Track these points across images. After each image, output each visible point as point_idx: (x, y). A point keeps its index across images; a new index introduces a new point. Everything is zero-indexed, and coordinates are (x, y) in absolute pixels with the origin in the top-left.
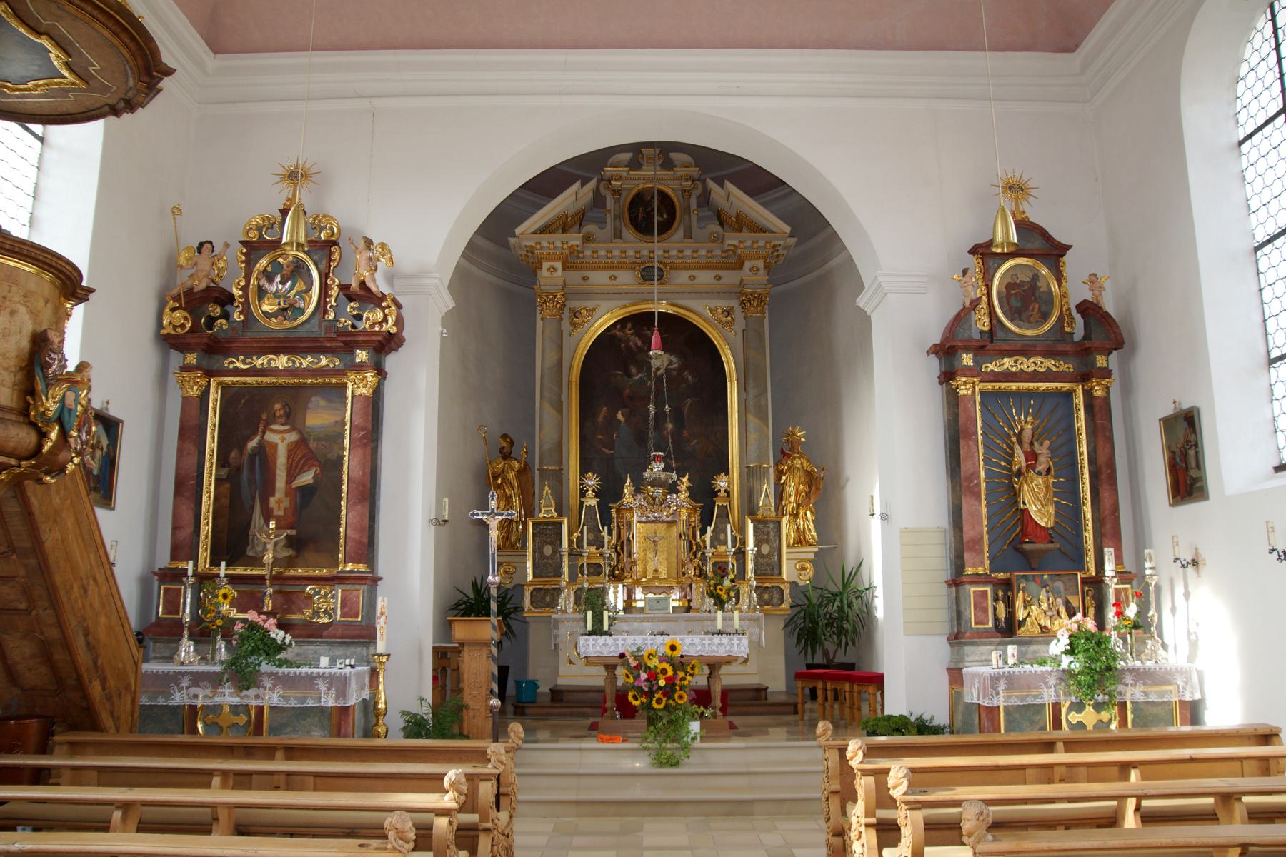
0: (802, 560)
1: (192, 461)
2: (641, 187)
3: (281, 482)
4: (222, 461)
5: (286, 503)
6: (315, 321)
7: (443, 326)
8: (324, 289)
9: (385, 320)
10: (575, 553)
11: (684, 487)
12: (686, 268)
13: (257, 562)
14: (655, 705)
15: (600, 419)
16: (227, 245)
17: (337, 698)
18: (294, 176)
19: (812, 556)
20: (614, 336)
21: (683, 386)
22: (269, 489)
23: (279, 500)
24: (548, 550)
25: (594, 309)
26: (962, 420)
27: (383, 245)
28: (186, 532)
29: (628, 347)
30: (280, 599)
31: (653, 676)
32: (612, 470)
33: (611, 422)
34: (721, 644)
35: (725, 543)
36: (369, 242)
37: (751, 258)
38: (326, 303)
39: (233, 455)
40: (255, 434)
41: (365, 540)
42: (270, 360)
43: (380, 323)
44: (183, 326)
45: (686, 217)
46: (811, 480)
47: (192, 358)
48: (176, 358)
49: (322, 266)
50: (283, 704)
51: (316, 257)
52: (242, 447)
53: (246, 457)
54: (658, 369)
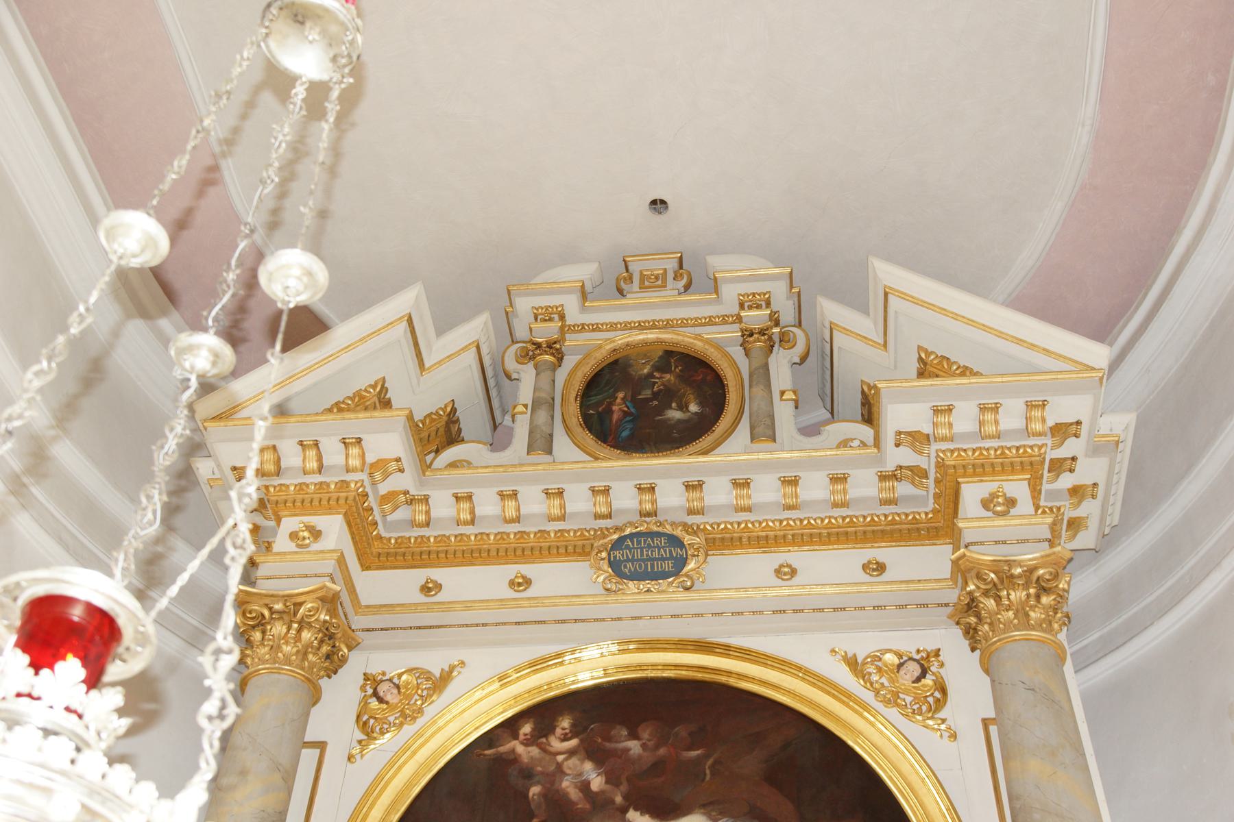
2: (622, 339)
12: (764, 541)
20: (511, 760)
29: (555, 800)
37: (981, 469)
45: (759, 391)
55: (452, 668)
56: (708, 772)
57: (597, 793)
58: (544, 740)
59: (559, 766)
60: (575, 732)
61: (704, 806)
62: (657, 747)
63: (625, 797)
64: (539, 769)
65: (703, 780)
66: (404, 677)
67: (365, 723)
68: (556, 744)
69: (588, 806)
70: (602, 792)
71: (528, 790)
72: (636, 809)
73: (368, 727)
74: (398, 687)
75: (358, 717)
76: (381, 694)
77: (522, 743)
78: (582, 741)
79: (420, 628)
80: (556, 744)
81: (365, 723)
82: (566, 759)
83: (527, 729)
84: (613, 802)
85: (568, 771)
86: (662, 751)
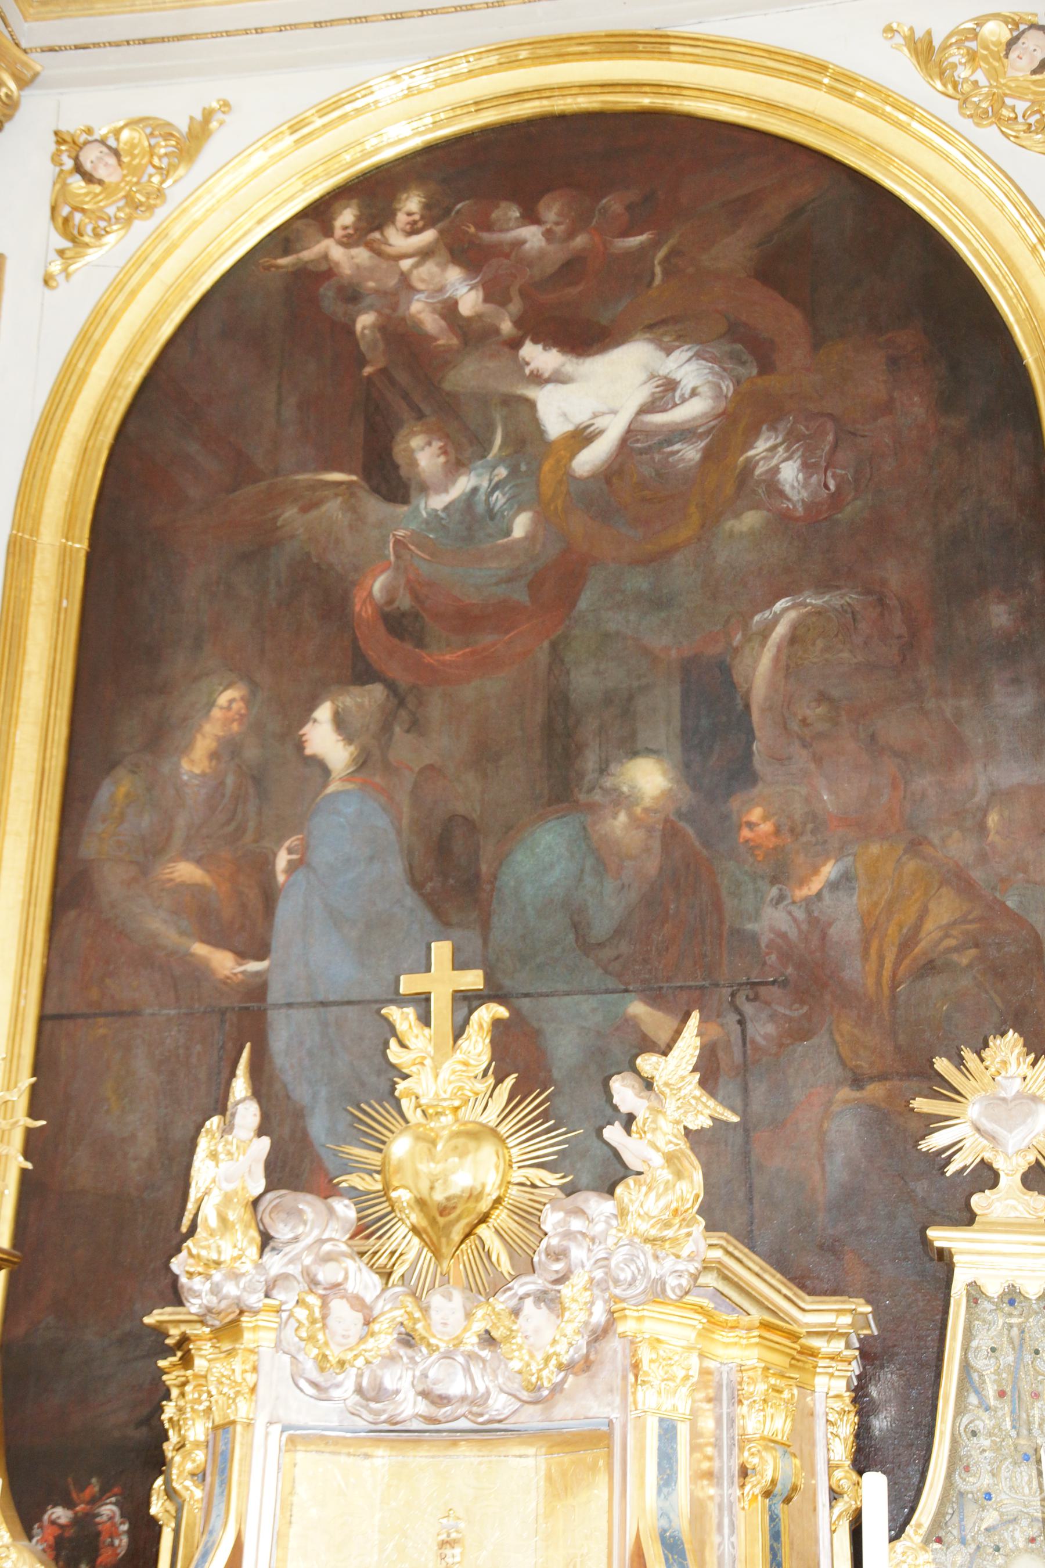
15: (195, 761)
20: (322, 273)
21: (751, 520)
25: (199, 133)
29: (401, 336)
33: (269, 780)
55: (208, 114)
56: (658, 270)
57: (469, 320)
58: (377, 235)
59: (405, 279)
60: (431, 216)
61: (650, 327)
62: (571, 235)
63: (518, 323)
64: (371, 284)
65: (650, 284)
66: (125, 135)
67: (66, 220)
68: (397, 240)
69: (455, 341)
70: (479, 316)
71: (354, 322)
72: (535, 341)
73: (72, 229)
74: (116, 153)
75: (54, 209)
76: (88, 166)
77: (341, 243)
78: (441, 232)
79: (144, 42)
81: (66, 220)
82: (416, 266)
83: (346, 217)
84: (497, 331)
85: (420, 286)
86: (580, 241)
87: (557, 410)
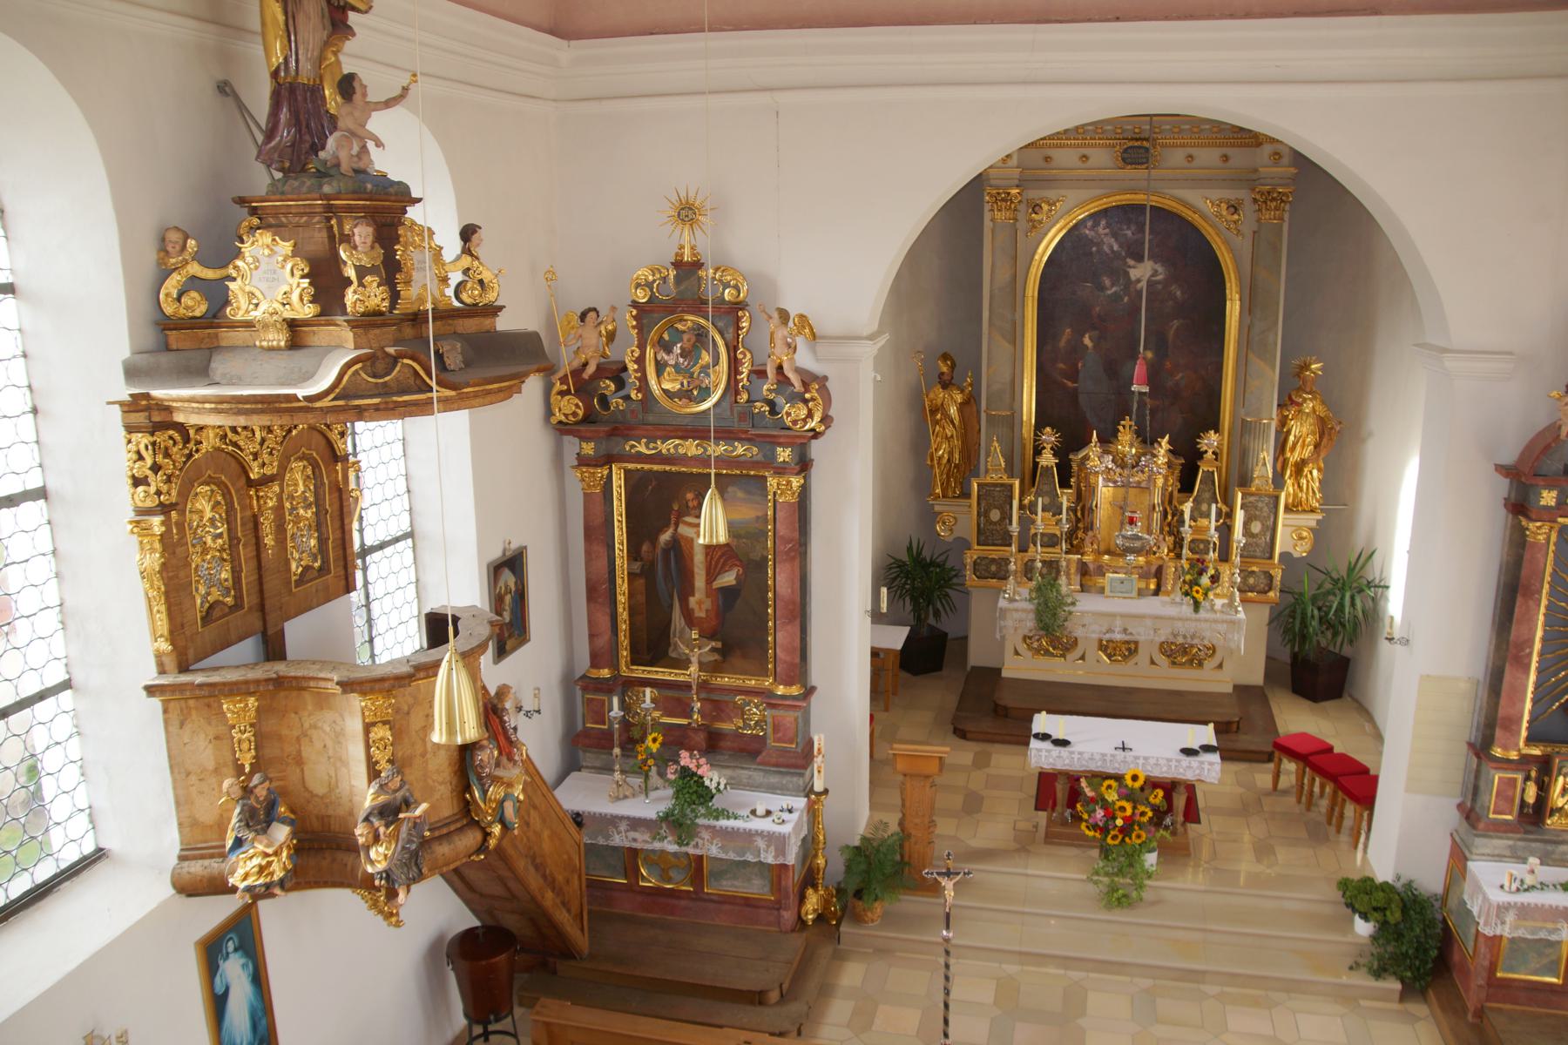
0: (1299, 528)
1: (602, 563)
3: (700, 582)
4: (634, 553)
5: (708, 604)
6: (725, 404)
7: (876, 370)
8: (734, 364)
9: (810, 415)
10: (1026, 523)
11: (1162, 452)
13: (683, 664)
14: (1109, 841)
15: (1062, 343)
16: (614, 309)
17: (776, 857)
18: (687, 213)
19: (1313, 524)
22: (687, 590)
23: (699, 600)
24: (995, 515)
26: (1524, 572)
27: (802, 317)
28: (603, 641)
30: (709, 706)
31: (1111, 816)
32: (1071, 420)
33: (1076, 349)
34: (1189, 767)
35: (1208, 516)
36: (784, 316)
38: (737, 382)
39: (645, 548)
40: (667, 526)
41: (798, 660)
42: (676, 447)
43: (804, 420)
44: (574, 414)
46: (1324, 430)
47: (589, 449)
48: (572, 446)
49: (729, 336)
50: (723, 856)
51: (720, 324)
52: (654, 541)
53: (659, 551)
54: (1139, 281)
60: (1108, 226)
68: (1101, 230)
80: (1101, 230)
87: (1134, 274)
